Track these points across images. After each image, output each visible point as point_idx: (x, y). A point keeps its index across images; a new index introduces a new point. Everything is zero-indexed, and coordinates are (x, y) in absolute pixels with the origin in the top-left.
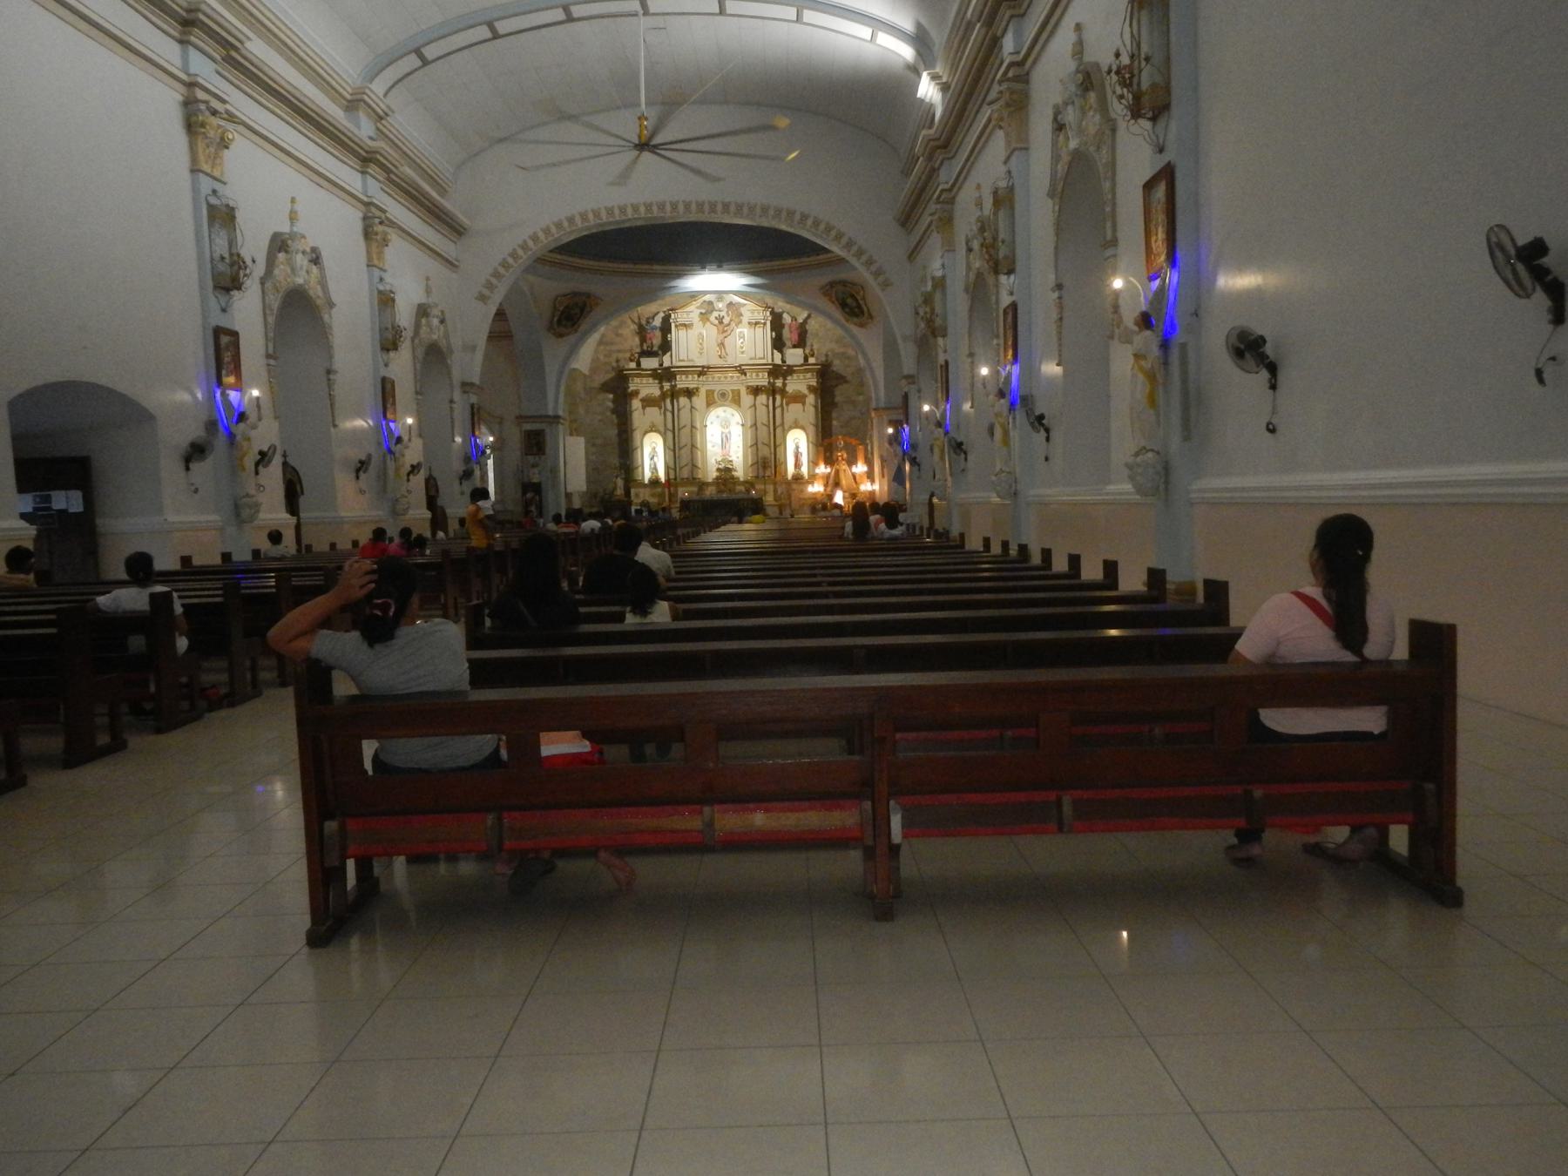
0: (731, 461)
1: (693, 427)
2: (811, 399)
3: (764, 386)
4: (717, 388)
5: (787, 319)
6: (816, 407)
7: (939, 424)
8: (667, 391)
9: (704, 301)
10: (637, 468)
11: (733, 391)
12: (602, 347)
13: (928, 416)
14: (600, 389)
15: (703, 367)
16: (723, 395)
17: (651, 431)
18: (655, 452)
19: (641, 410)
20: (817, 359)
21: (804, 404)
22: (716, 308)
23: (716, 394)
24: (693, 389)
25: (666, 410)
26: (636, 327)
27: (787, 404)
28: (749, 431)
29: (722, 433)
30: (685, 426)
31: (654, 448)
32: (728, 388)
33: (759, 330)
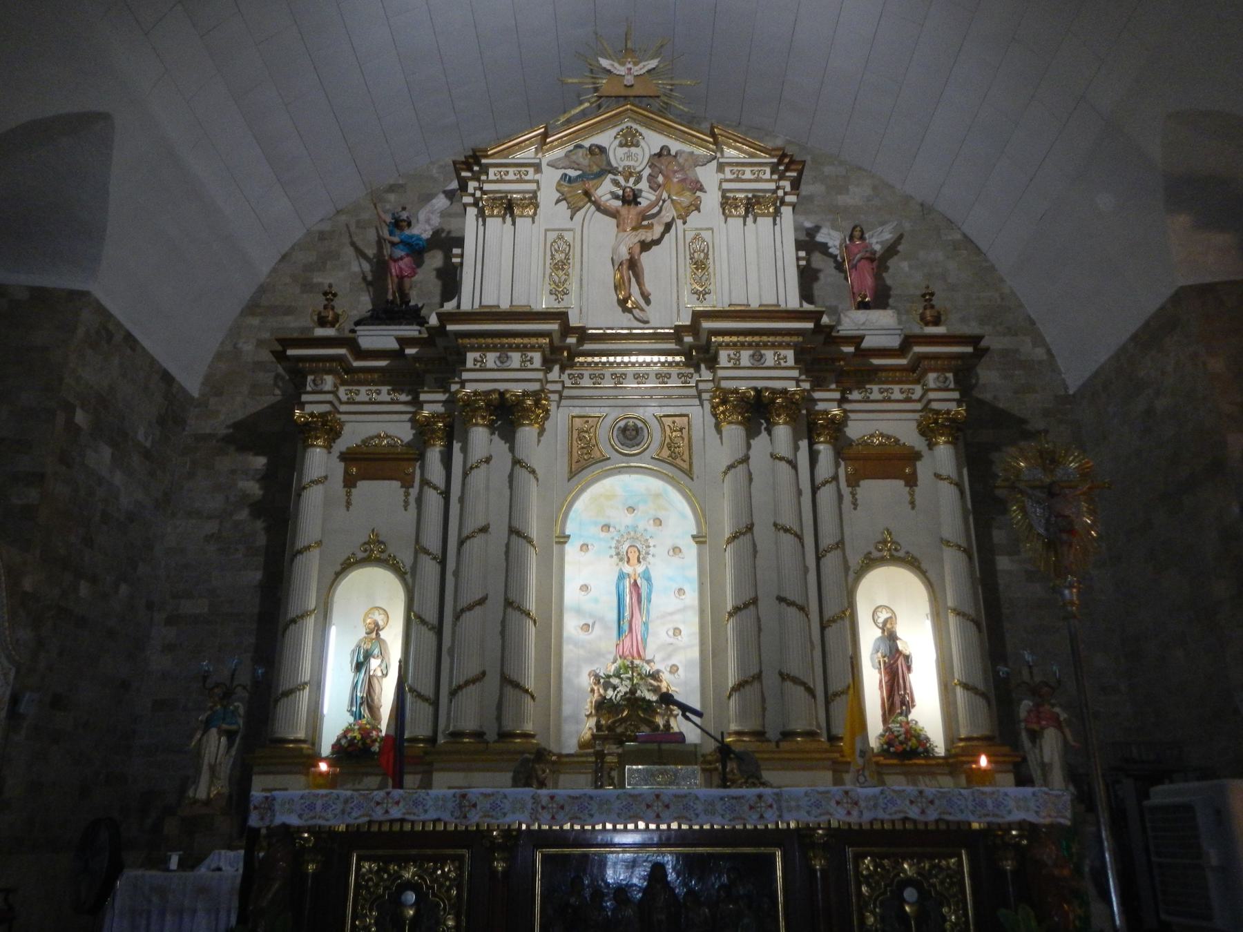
0: (655, 676)
1: (514, 532)
2: (943, 456)
4: (608, 416)
5: (832, 238)
6: (959, 485)
8: (435, 416)
9: (580, 146)
10: (288, 693)
11: (659, 419)
12: (255, 321)
14: (228, 440)
16: (631, 434)
17: (367, 561)
20: (948, 330)
21: (911, 481)
22: (614, 164)
24: (526, 394)
25: (425, 482)
26: (367, 267)
27: (853, 482)
28: (728, 556)
29: (622, 576)
30: (484, 530)
31: (376, 629)
32: (649, 413)
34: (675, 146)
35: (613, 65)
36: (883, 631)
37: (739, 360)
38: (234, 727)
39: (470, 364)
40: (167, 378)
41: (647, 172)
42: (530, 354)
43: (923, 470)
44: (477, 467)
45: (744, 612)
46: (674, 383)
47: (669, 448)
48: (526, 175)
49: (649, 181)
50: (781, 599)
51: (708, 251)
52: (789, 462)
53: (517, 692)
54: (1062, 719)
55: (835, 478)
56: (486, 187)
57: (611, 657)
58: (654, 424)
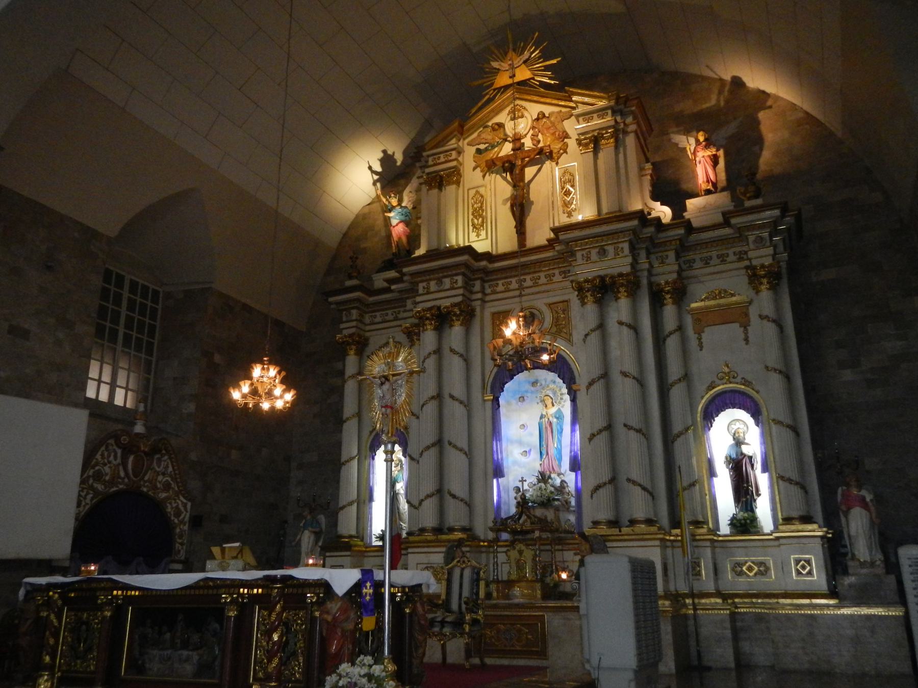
3: (621, 275)
11: (549, 305)
15: (469, 250)
24: (454, 305)
29: (542, 417)
34: (547, 110)
35: (500, 65)
36: (734, 439)
37: (590, 258)
38: (317, 530)
39: (421, 291)
40: (278, 323)
41: (531, 132)
42: (456, 278)
43: (753, 312)
44: (428, 357)
45: (598, 436)
46: (558, 278)
47: (556, 326)
48: (450, 156)
49: (532, 139)
50: (625, 425)
51: (574, 180)
52: (629, 326)
53: (455, 499)
54: (868, 499)
55: (680, 328)
56: (427, 170)
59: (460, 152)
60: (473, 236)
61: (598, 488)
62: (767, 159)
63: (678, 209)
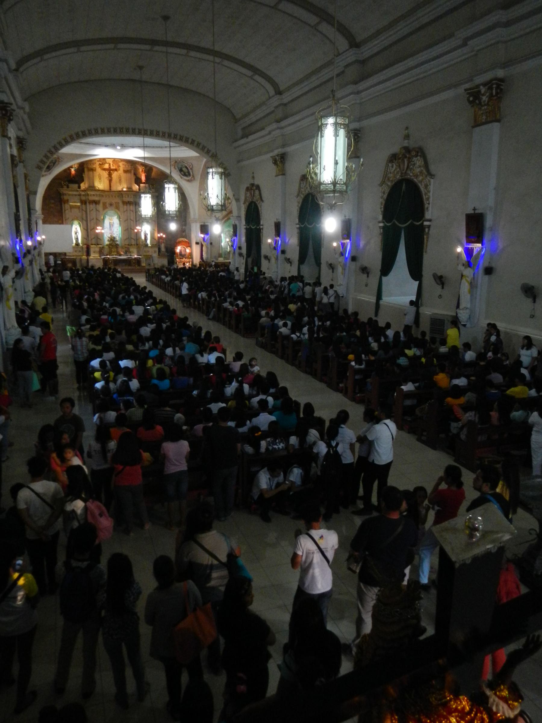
3: (131, 202)
7: (275, 248)
11: (116, 203)
13: (270, 244)
18: (77, 230)
19: (69, 209)
23: (107, 203)
24: (97, 201)
25: (82, 210)
29: (110, 223)
30: (93, 219)
33: (128, 175)
46: (117, 197)
56: (89, 166)
57: (109, 233)
58: (114, 203)
59: (96, 163)
60: (99, 184)
61: (126, 239)
62: (153, 174)
63: (139, 186)
